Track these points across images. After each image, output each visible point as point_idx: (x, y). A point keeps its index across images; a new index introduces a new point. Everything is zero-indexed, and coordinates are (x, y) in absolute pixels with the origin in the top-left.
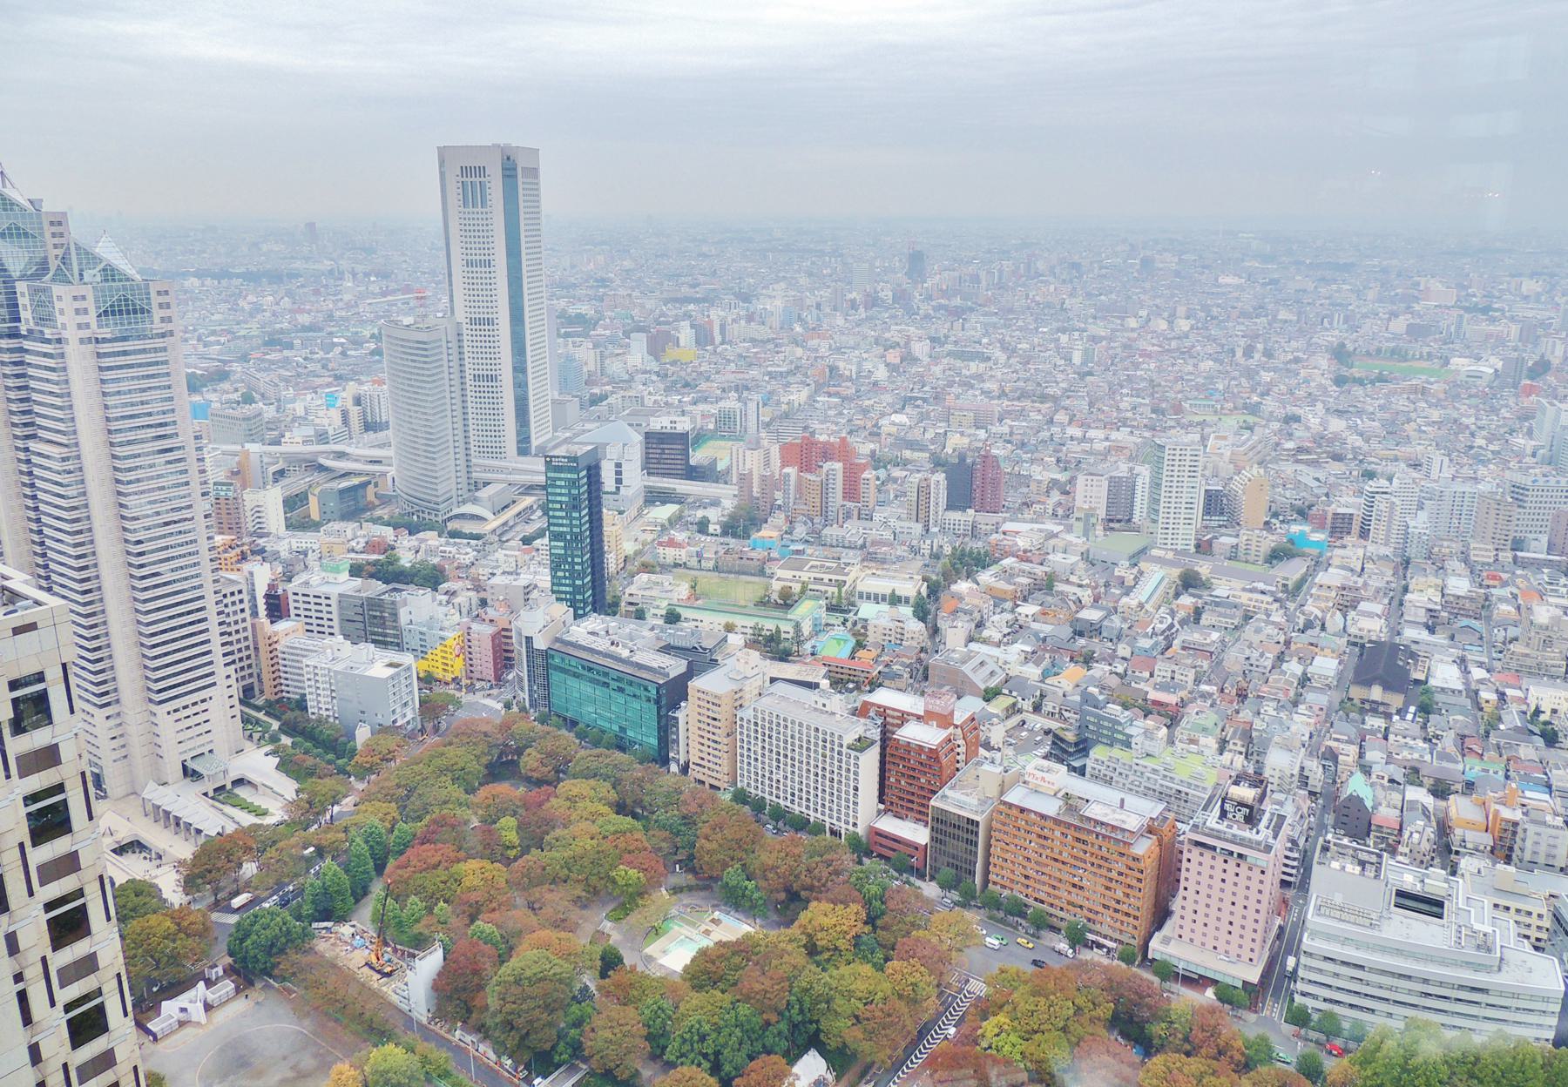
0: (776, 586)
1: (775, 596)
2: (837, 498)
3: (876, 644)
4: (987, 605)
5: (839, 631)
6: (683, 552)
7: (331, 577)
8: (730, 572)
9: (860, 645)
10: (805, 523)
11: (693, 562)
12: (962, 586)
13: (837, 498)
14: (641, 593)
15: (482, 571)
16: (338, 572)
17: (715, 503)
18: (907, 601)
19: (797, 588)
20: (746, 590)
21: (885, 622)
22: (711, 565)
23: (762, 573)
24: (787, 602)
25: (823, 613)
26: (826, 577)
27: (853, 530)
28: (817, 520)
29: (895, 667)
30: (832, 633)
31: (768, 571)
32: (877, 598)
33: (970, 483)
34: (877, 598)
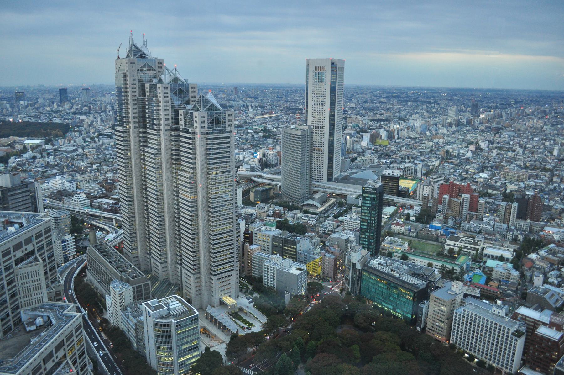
0: (447, 247)
1: (446, 252)
2: (466, 210)
3: (497, 279)
4: (547, 267)
5: (478, 271)
6: (403, 228)
7: (269, 228)
8: (423, 239)
9: (489, 279)
10: (453, 220)
11: (407, 233)
12: (533, 256)
13: (466, 210)
14: (389, 246)
15: (321, 230)
16: (272, 226)
17: (412, 207)
18: (507, 260)
19: (456, 249)
20: (431, 247)
21: (500, 270)
22: (414, 235)
23: (437, 240)
24: (452, 256)
25: (470, 262)
26: (470, 246)
27: (474, 224)
28: (458, 218)
29: (508, 292)
30: (475, 272)
31: (440, 240)
32: (494, 258)
33: (528, 208)
34: (494, 258)
